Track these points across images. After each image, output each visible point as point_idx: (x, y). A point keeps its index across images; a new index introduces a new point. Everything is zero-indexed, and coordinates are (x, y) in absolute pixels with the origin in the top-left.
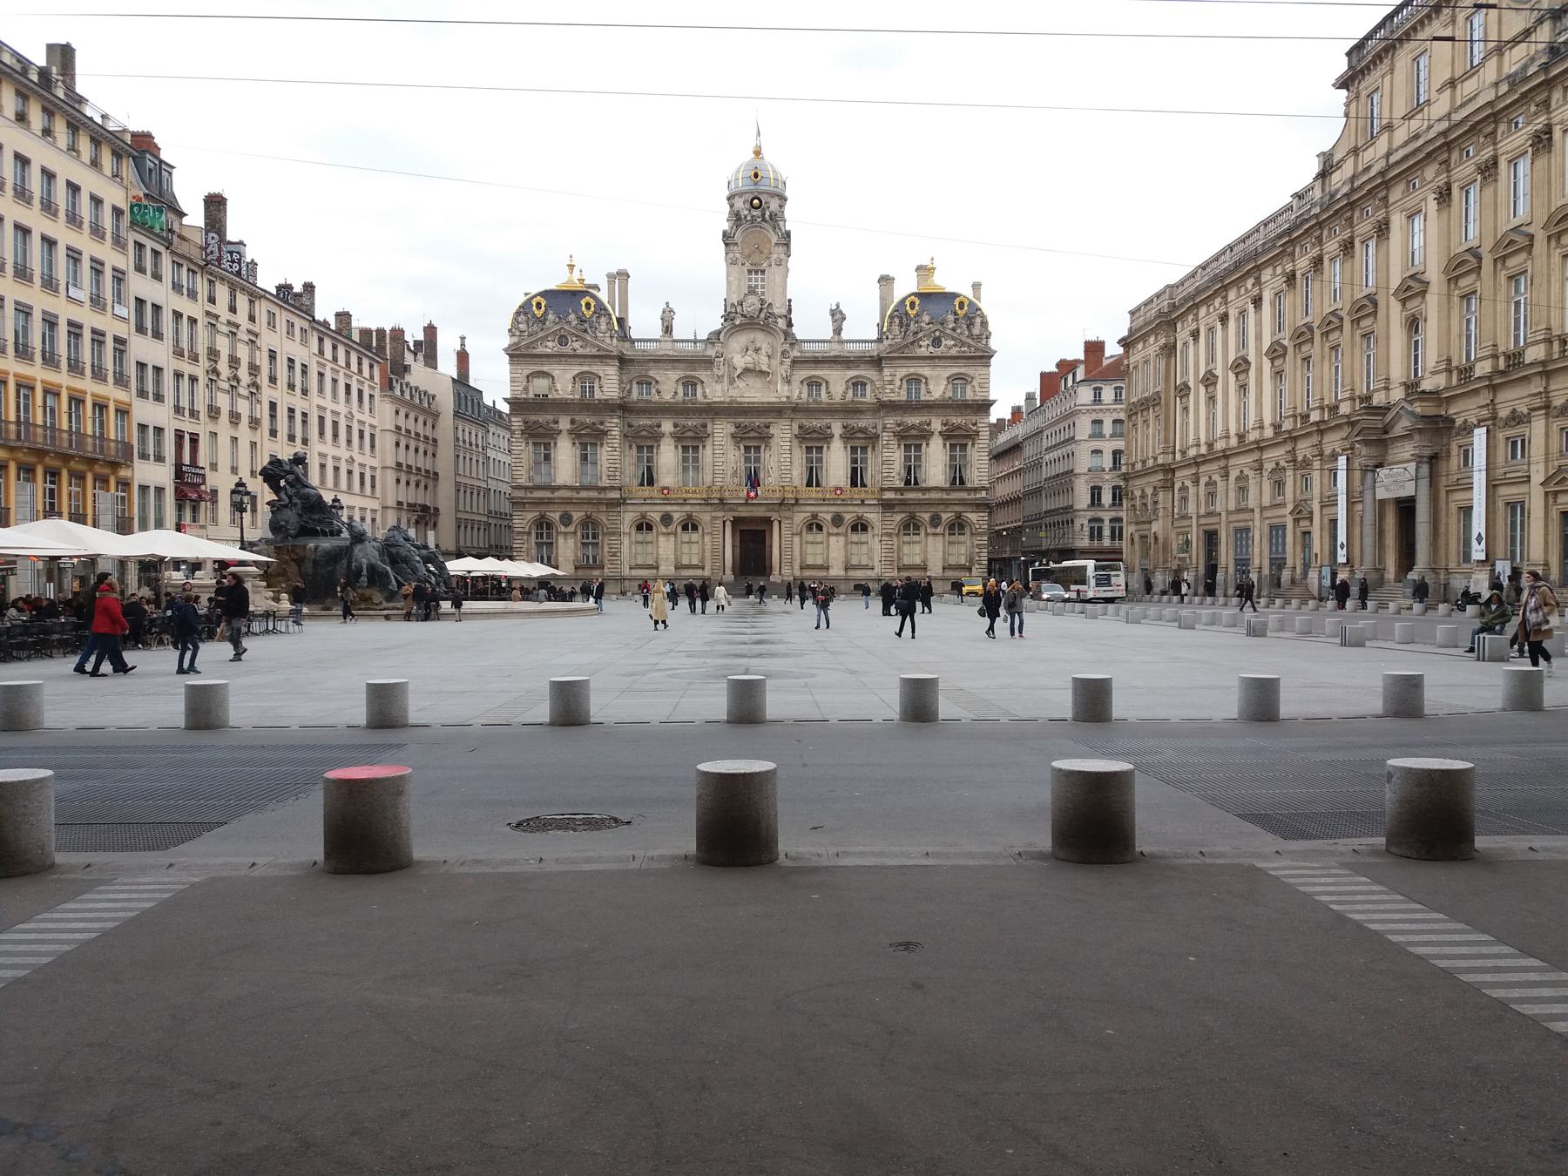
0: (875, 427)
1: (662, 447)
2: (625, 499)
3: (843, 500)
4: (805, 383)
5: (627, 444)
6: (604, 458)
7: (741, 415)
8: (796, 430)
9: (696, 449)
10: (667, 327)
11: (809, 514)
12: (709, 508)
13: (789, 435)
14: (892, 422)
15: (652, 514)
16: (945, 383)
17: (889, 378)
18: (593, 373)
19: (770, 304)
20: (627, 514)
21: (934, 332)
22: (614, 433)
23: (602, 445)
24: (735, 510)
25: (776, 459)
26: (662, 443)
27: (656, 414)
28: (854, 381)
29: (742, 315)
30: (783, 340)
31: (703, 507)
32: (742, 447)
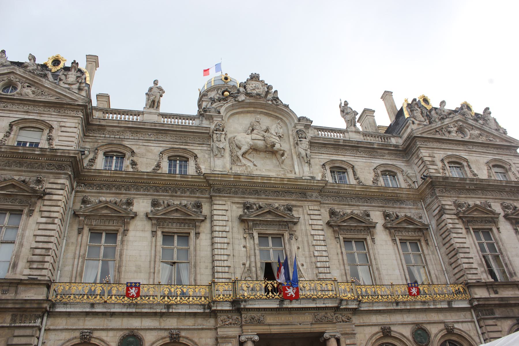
0: (421, 218)
1: (132, 234)
2: (53, 305)
3: (424, 303)
4: (327, 167)
5: (76, 227)
6: (29, 233)
7: (250, 193)
8: (326, 217)
9: (185, 237)
10: (153, 102)
11: (377, 329)
12: (211, 323)
13: (320, 222)
14: (450, 203)
15: (103, 335)
16: (486, 168)
17: (430, 159)
18: (43, 122)
19: (276, 92)
20: (52, 336)
21: (457, 121)
22: (55, 197)
23: (31, 213)
24: (260, 322)
25: (307, 253)
26: (131, 227)
27: (128, 189)
28: (382, 169)
29: (247, 94)
30: (296, 121)
31: (200, 322)
32: (256, 236)
